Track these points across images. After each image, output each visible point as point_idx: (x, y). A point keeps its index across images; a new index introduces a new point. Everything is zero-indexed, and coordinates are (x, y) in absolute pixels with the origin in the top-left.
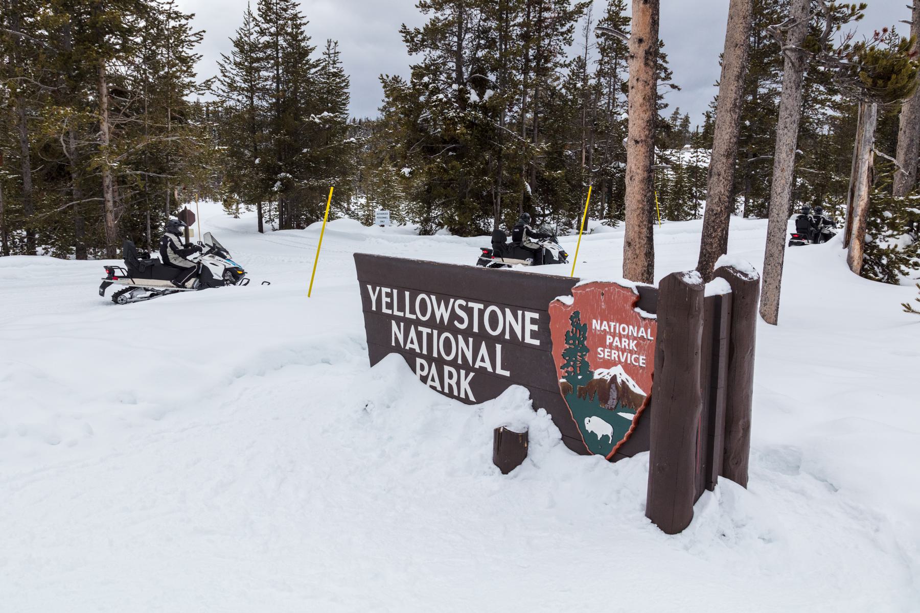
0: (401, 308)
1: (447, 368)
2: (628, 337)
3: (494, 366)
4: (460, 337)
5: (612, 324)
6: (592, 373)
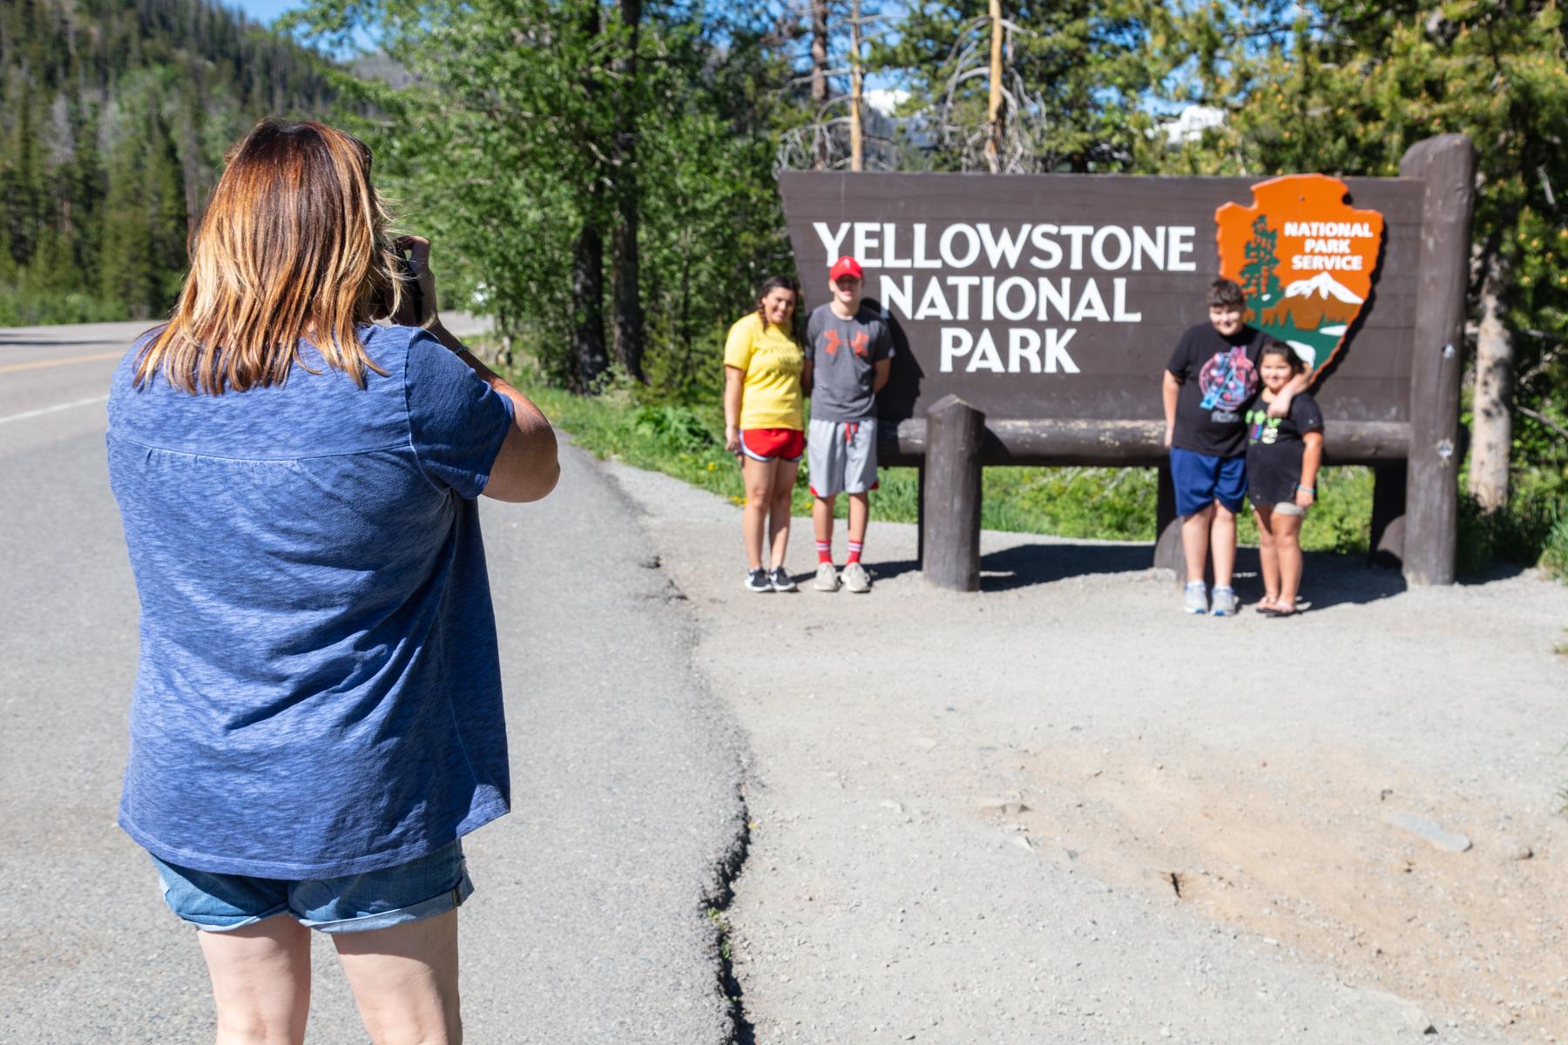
0: (904, 249)
1: (1015, 335)
2: (1336, 237)
3: (1110, 309)
4: (1044, 283)
6: (1283, 291)
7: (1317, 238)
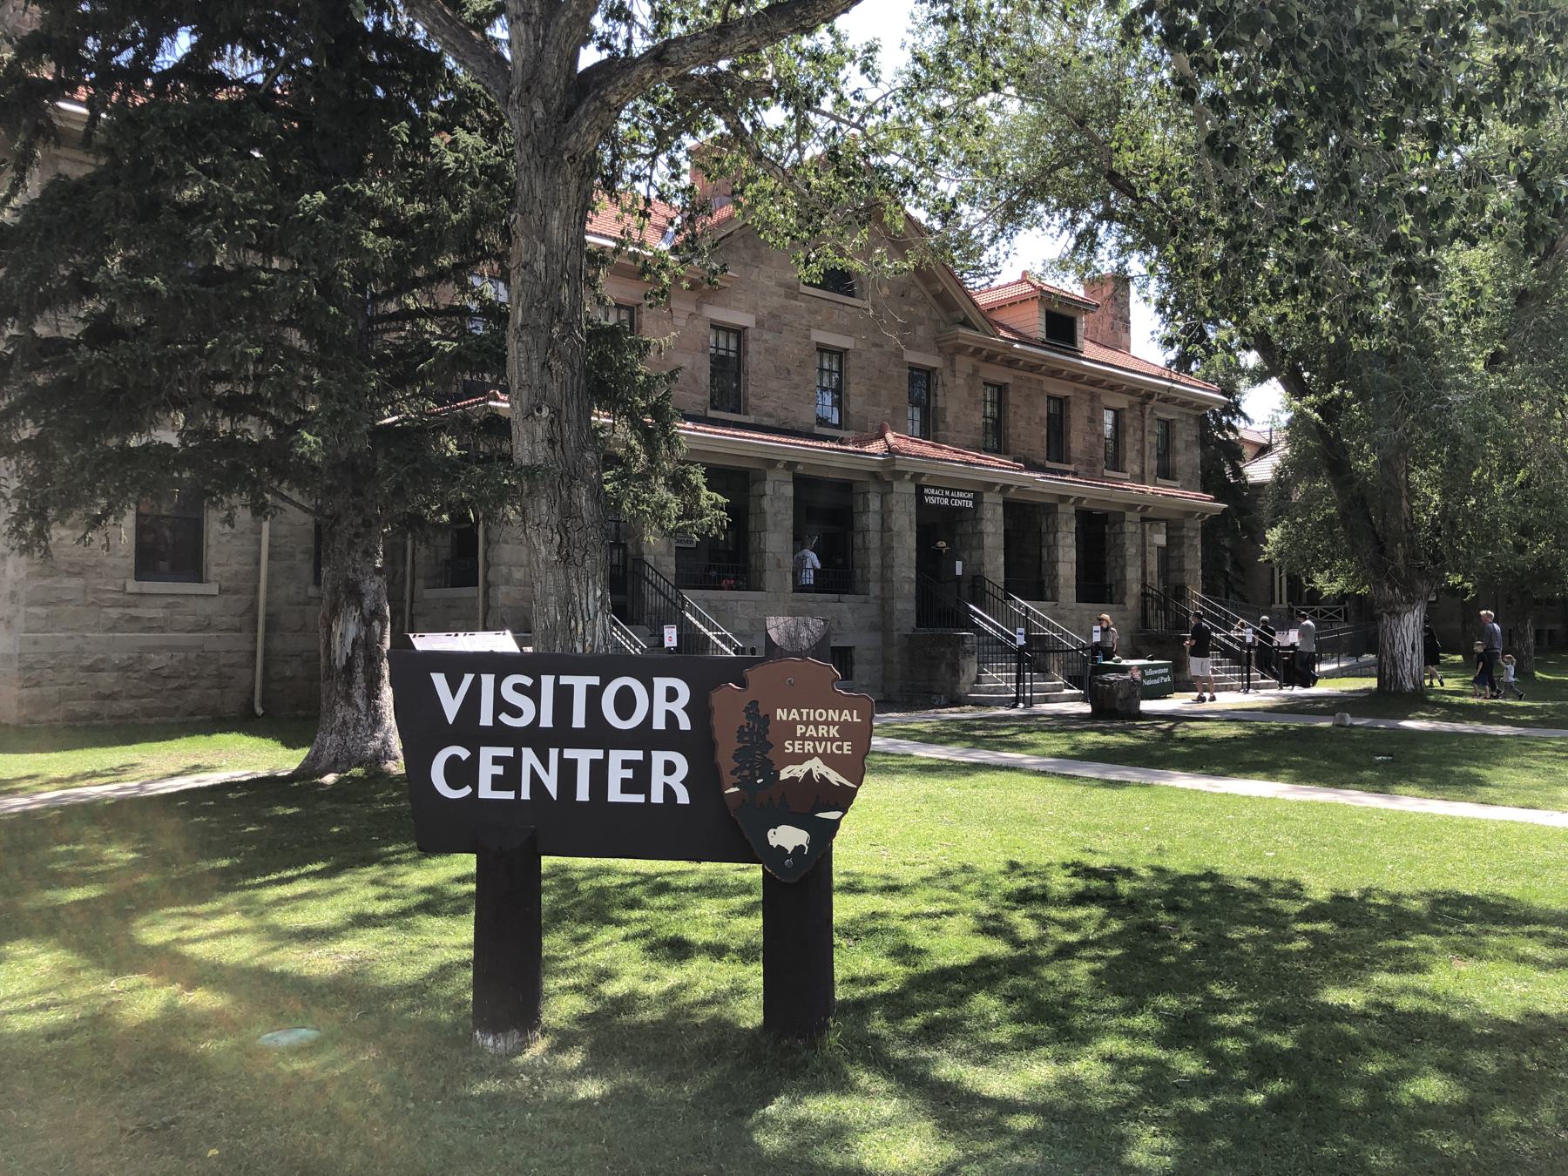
2: (826, 723)
5: (805, 711)
7: (807, 724)
